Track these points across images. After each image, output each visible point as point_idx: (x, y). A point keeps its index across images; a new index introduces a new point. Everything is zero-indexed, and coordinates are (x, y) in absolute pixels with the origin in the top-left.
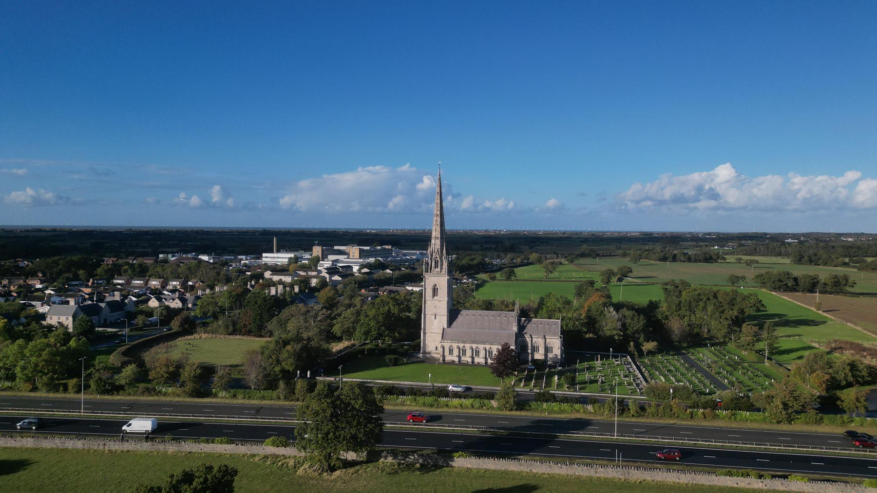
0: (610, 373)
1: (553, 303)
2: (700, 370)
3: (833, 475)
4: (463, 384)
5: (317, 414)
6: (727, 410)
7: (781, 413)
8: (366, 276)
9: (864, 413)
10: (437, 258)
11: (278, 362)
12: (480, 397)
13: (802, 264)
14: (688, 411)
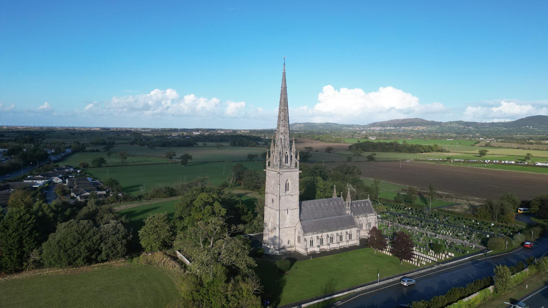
10: (287, 153)
13: (236, 146)
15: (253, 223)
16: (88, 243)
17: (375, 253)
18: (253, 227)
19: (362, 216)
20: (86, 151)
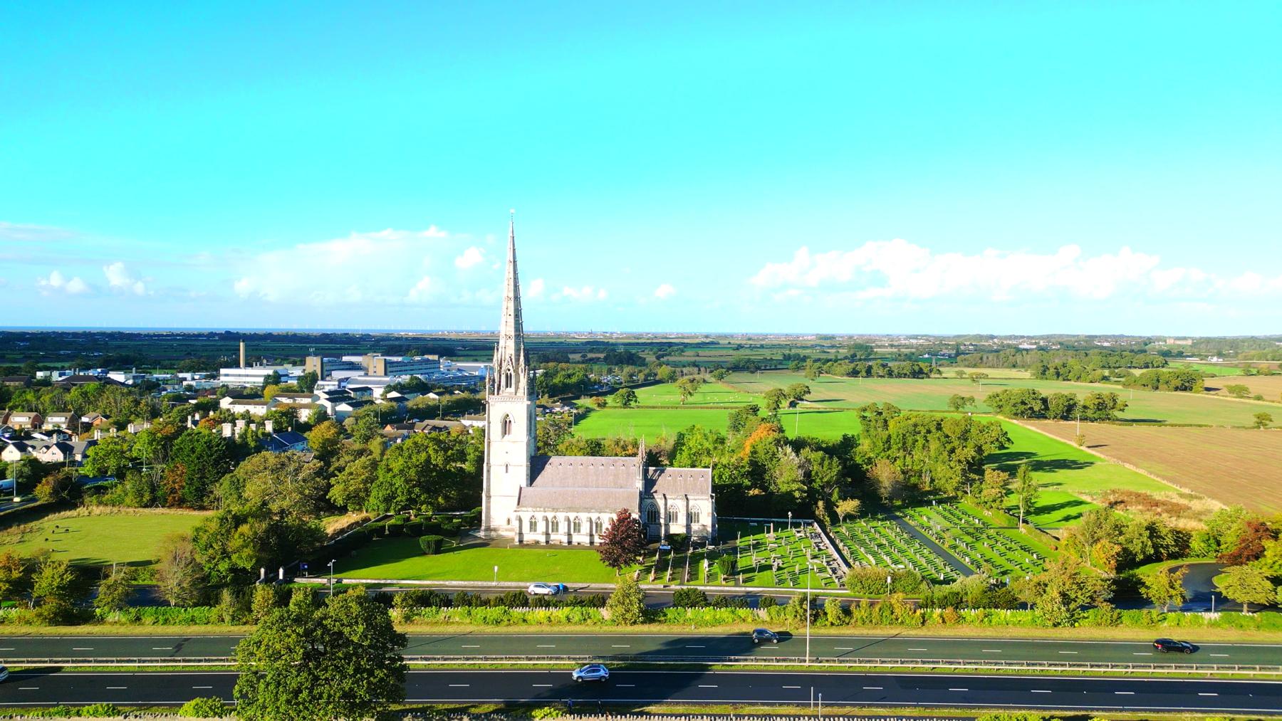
0: (790, 552)
1: (698, 442)
2: (926, 542)
3: (1150, 711)
4: (551, 582)
5: (276, 656)
6: (978, 608)
7: (1060, 609)
8: (394, 404)
9: (1181, 605)
10: (509, 370)
11: (225, 554)
12: (581, 603)
13: (1047, 379)
14: (919, 612)
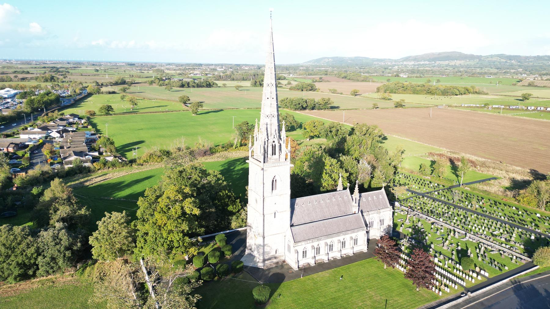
10: (274, 142)
15: (241, 215)
16: (21, 258)
17: (385, 268)
18: (240, 220)
19: (372, 213)
20: (102, 93)
